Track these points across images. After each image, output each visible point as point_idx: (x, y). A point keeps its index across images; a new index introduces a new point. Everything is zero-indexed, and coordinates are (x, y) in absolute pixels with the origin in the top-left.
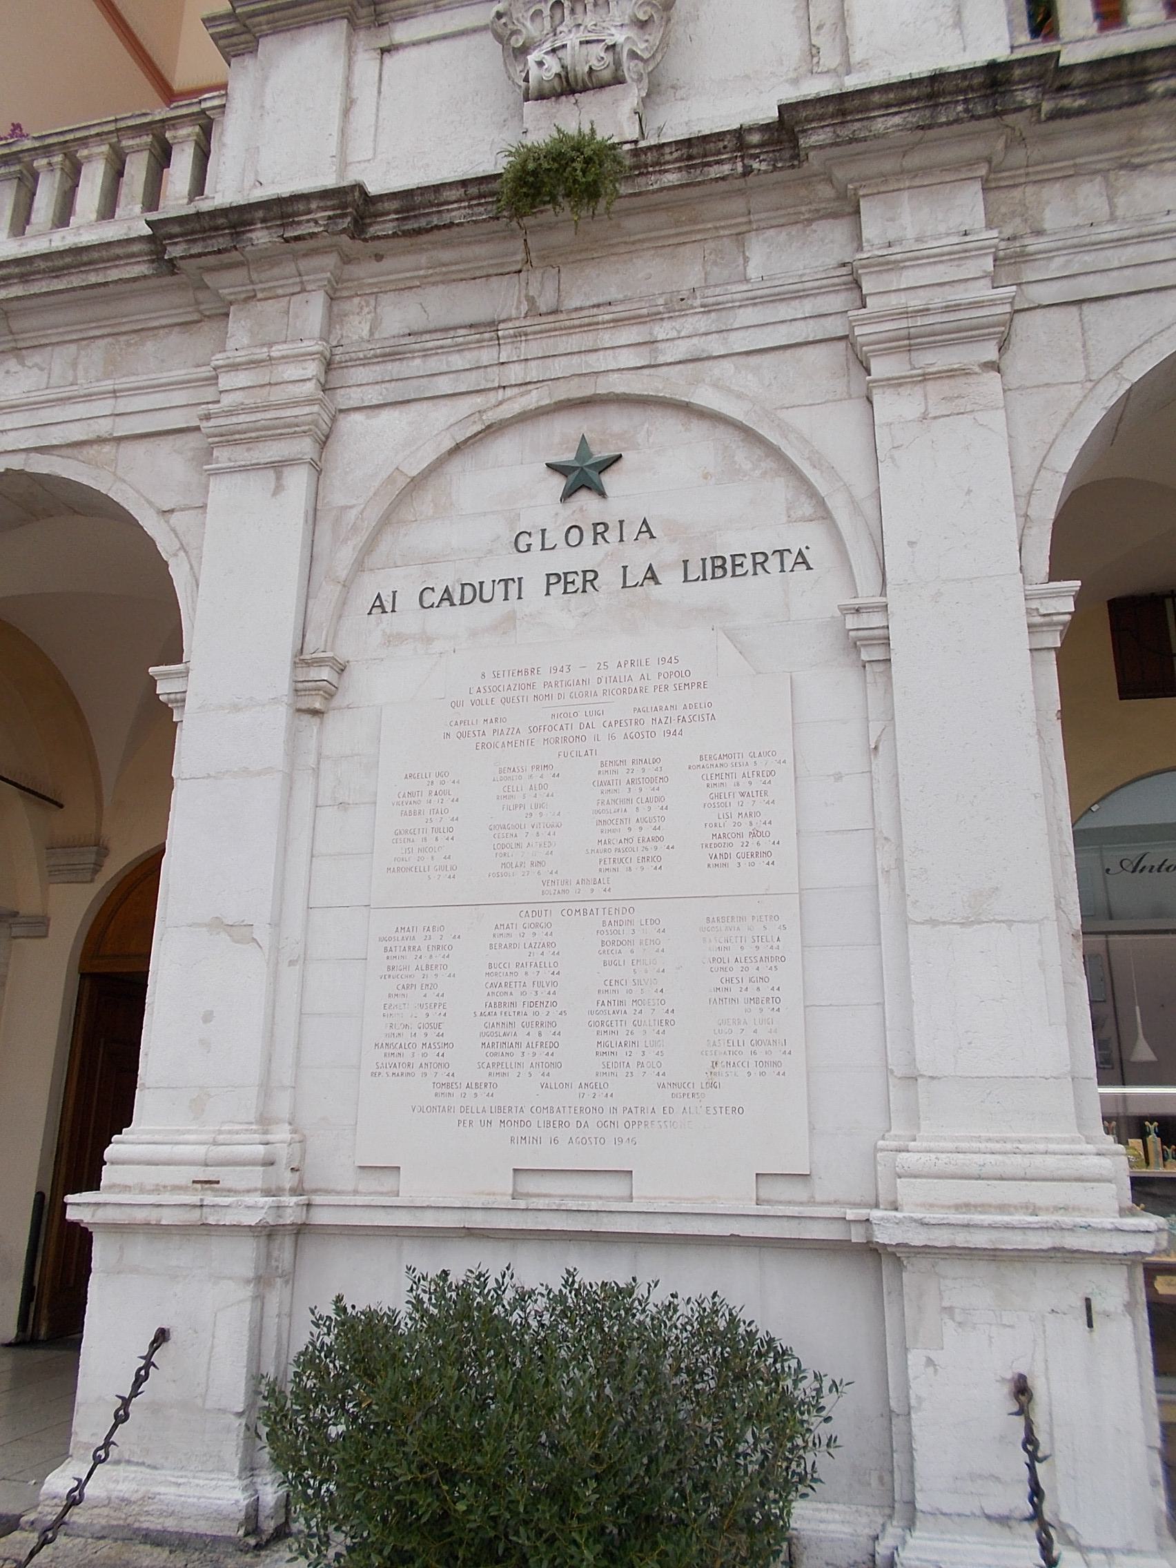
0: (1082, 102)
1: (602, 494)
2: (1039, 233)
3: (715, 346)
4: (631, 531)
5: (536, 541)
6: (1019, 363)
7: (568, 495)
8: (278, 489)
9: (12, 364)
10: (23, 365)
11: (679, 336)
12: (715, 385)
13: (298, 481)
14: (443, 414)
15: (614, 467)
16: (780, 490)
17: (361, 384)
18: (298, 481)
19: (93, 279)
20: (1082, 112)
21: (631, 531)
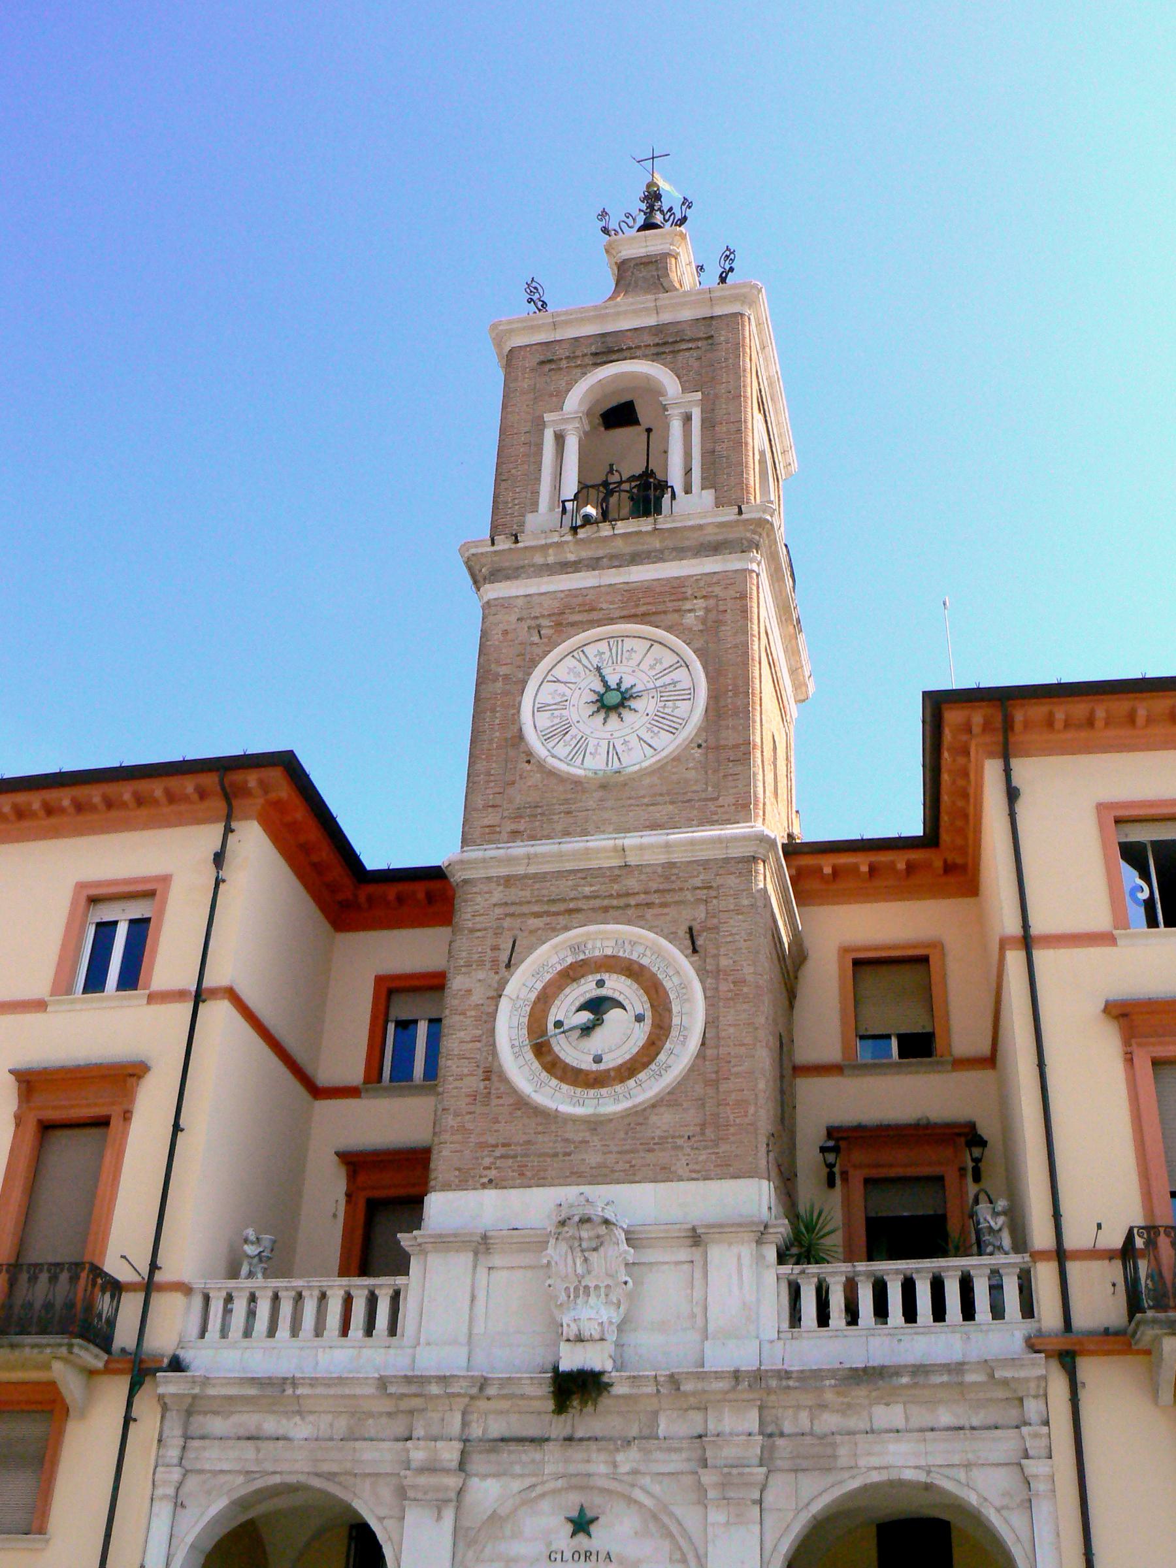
0: (797, 1384)
1: (589, 1535)
2: (782, 1435)
3: (643, 1468)
4: (602, 1556)
5: (559, 1557)
6: (769, 1498)
7: (574, 1534)
8: (439, 1518)
9: (297, 1419)
10: (303, 1419)
11: (627, 1460)
12: (641, 1488)
13: (449, 1514)
14: (516, 1485)
15: (596, 1523)
16: (666, 1545)
17: (478, 1463)
18: (449, 1514)
19: (347, 1391)
20: (796, 1388)
21: (602, 1556)
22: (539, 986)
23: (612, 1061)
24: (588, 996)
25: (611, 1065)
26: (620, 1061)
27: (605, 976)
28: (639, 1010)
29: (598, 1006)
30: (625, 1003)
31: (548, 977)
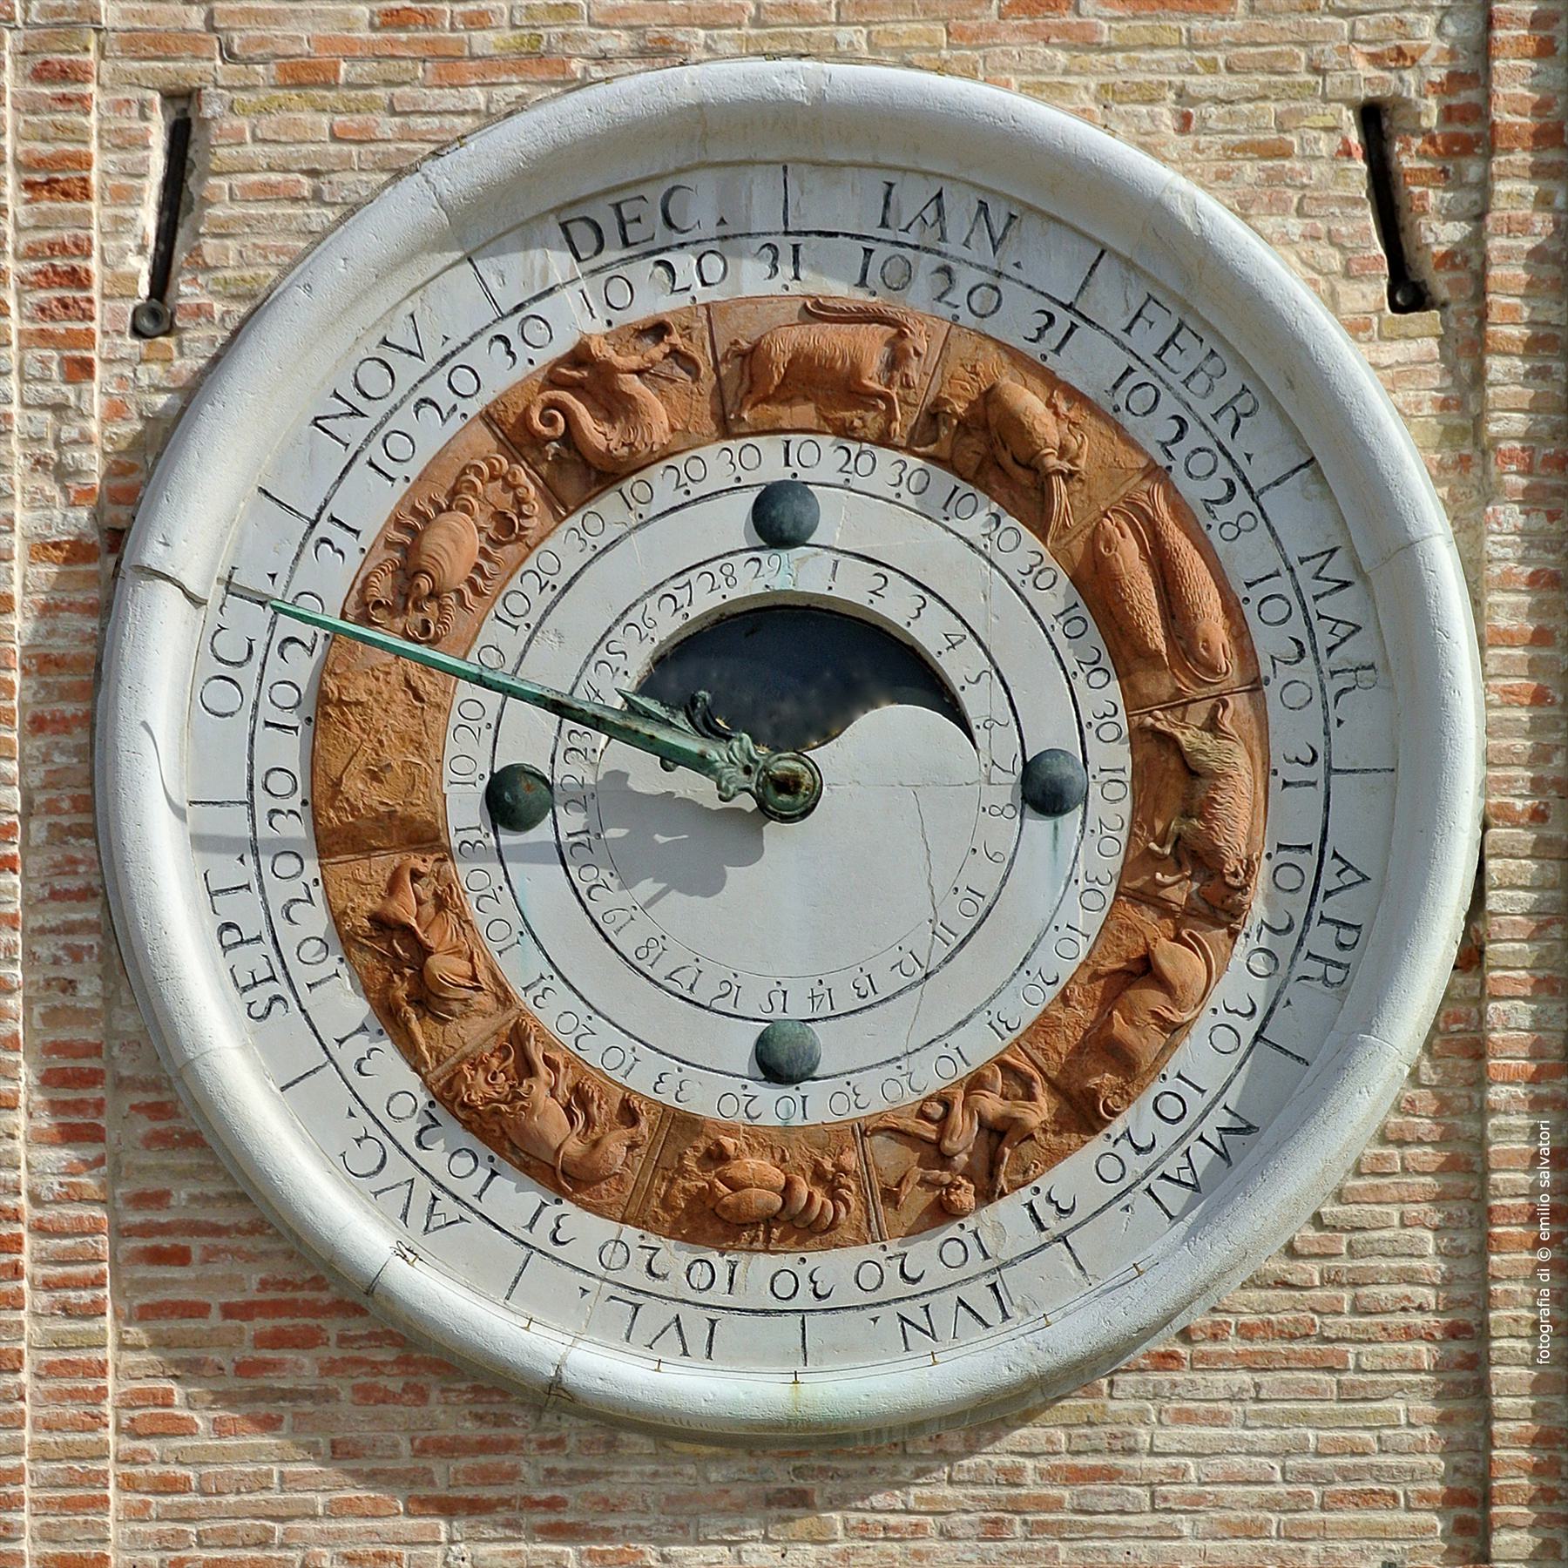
22: (372, 505)
23: (874, 1072)
24: (705, 600)
25: (881, 1095)
26: (932, 1075)
27: (818, 459)
28: (1051, 730)
29: (785, 676)
30: (958, 666)
31: (432, 434)
